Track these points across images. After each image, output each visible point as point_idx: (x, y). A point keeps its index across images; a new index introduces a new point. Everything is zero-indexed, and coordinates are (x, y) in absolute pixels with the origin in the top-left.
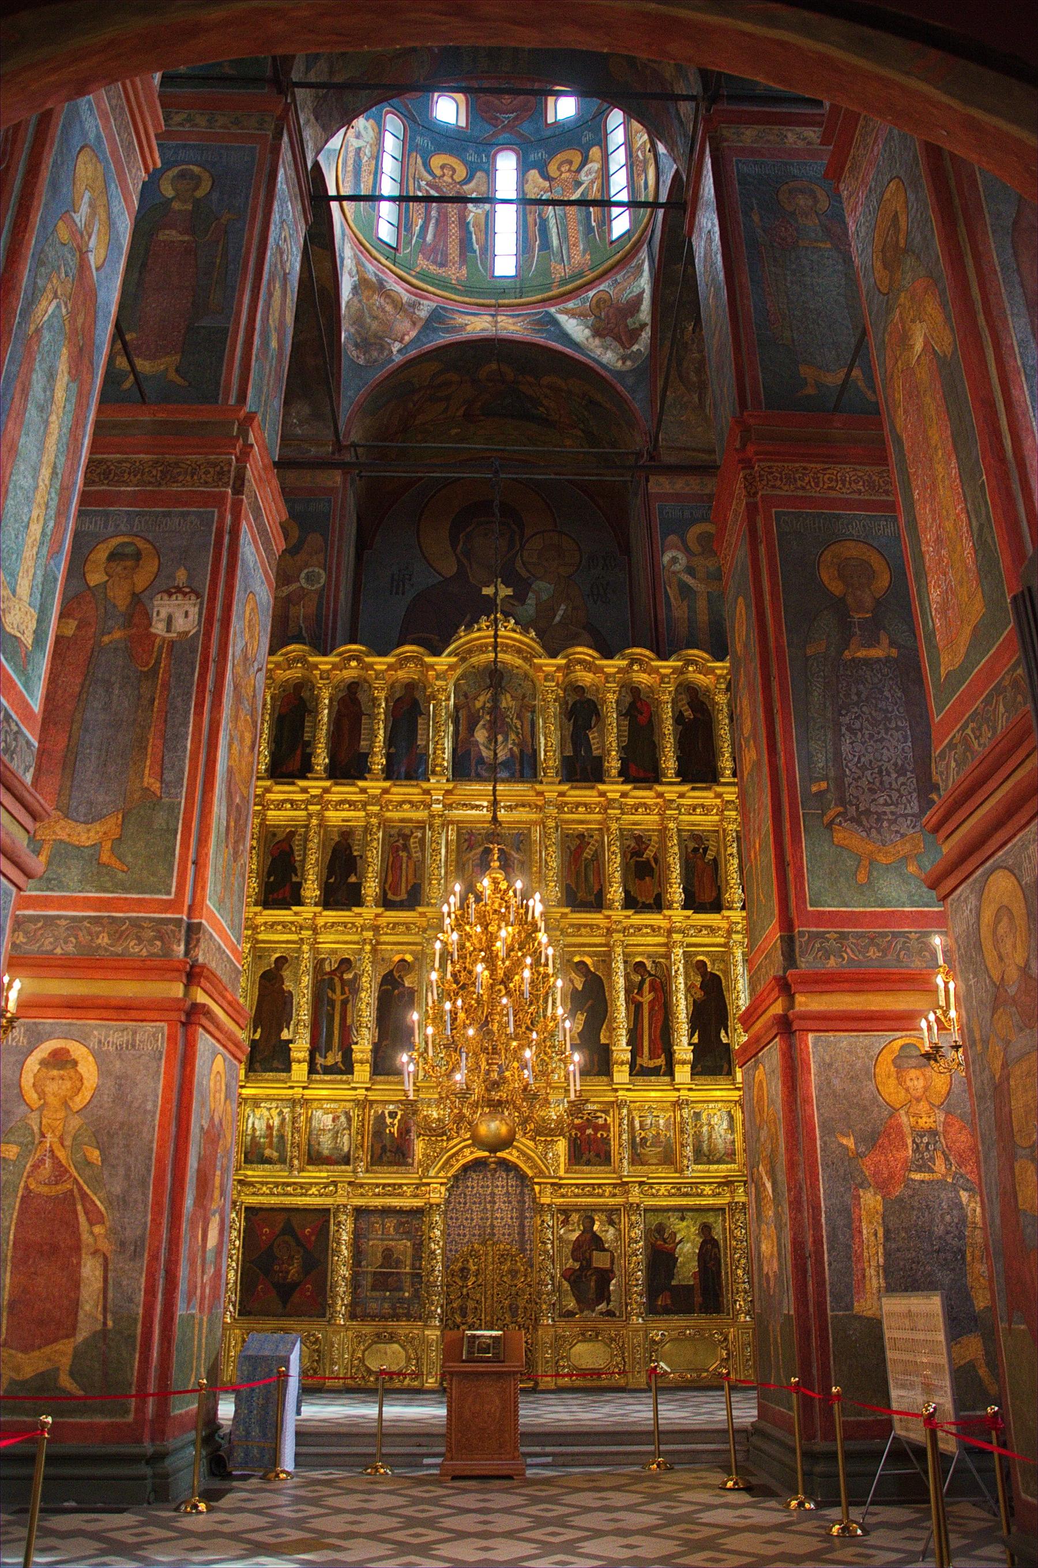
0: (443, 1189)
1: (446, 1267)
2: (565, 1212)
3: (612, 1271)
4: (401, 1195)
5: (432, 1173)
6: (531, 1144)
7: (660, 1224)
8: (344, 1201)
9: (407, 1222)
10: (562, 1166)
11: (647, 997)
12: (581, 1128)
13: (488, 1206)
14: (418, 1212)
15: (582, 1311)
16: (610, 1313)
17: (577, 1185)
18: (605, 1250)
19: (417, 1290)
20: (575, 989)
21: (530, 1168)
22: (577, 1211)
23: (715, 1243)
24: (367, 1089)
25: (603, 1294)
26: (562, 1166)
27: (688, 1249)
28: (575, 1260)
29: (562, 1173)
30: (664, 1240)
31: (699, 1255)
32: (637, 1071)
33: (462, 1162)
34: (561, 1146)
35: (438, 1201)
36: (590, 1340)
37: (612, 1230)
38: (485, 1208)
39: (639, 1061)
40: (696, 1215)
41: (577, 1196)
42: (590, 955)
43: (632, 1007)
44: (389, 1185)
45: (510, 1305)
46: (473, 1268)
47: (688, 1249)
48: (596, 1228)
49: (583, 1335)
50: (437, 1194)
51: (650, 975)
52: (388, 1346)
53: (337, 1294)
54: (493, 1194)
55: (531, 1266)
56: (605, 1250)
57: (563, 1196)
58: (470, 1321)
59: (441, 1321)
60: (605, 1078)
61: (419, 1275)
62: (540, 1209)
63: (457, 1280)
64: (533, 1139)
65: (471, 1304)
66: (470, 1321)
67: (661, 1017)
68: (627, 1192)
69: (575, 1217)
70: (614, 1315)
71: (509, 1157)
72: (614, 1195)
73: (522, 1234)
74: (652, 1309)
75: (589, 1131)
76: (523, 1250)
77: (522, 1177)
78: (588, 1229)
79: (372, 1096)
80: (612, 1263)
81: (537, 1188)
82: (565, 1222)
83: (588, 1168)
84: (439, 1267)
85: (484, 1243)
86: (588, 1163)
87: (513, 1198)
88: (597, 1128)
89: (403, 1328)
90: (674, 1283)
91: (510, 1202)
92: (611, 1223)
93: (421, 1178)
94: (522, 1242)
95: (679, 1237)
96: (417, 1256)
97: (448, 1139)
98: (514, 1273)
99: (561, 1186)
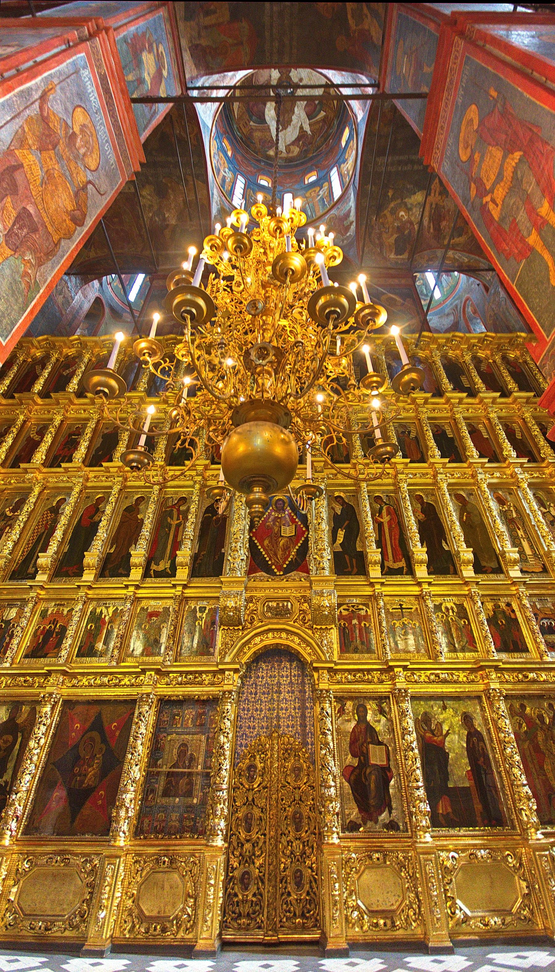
0: (236, 676)
1: (234, 765)
2: (340, 699)
3: (389, 769)
4: (201, 683)
5: (228, 659)
6: (310, 632)
7: (426, 713)
8: (149, 690)
9: (204, 713)
10: (335, 653)
11: (385, 519)
12: (348, 619)
13: (275, 696)
14: (213, 702)
15: (365, 824)
16: (392, 826)
17: (349, 671)
18: (380, 743)
19: (205, 795)
20: (336, 515)
21: (309, 654)
22: (351, 698)
23: (479, 735)
24: (185, 587)
25: (385, 803)
26: (335, 653)
27: (455, 743)
28: (354, 756)
29: (335, 659)
30: (432, 732)
31: (468, 749)
32: (387, 571)
33: (253, 650)
34: (334, 635)
35: (230, 687)
36: (378, 866)
37: (383, 719)
38: (272, 698)
39: (386, 564)
40: (455, 704)
41: (349, 682)
42: (345, 492)
43: (377, 525)
44: (191, 673)
45: (294, 817)
46: (260, 766)
47: (455, 743)
48: (369, 718)
49: (370, 857)
50: (232, 682)
51: (386, 504)
52: (166, 876)
53: (123, 805)
54: (279, 684)
55: (313, 763)
56: (380, 743)
57: (339, 683)
58: (254, 837)
59: (225, 840)
60: (362, 578)
61: (208, 774)
62: (319, 696)
63: (244, 780)
64: (311, 628)
65: (257, 812)
66: (254, 837)
67: (397, 532)
68: (393, 679)
69: (349, 705)
70: (397, 828)
71: (292, 645)
72: (381, 682)
73: (303, 725)
74: (436, 821)
75: (355, 622)
76: (305, 744)
77: (302, 664)
78: (362, 719)
79: (189, 592)
80: (388, 759)
81: (316, 675)
82: (342, 711)
83: (357, 655)
84: (226, 765)
85: (270, 737)
86: (356, 651)
87: (295, 688)
88: (360, 619)
89: (185, 846)
90: (451, 785)
91: (293, 692)
92: (382, 712)
93: (217, 665)
94: (304, 735)
95: (445, 728)
96: (209, 754)
97: (243, 629)
98: (297, 770)
99: (336, 671)
